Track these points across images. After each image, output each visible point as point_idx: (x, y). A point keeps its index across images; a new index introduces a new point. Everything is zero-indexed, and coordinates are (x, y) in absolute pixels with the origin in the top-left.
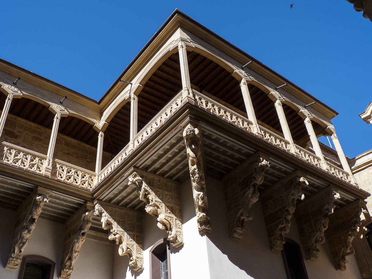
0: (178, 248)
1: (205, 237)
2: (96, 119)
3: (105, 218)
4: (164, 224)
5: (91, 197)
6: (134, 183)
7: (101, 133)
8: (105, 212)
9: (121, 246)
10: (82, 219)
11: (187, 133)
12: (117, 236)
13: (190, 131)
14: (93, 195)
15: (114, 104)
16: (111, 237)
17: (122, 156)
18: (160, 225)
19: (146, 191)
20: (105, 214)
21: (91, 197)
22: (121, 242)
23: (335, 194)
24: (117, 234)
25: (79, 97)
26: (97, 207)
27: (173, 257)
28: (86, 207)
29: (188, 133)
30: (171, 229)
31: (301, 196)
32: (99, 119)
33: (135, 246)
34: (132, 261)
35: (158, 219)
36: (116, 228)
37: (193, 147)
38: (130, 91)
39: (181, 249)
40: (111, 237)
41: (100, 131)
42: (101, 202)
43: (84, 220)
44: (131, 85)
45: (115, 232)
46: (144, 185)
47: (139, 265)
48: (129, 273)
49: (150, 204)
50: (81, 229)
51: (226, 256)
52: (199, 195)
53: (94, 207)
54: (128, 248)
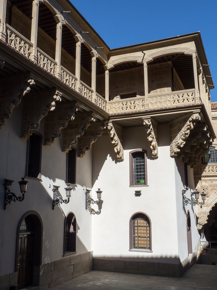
0: (155, 157)
1: (173, 159)
2: (106, 61)
3: (113, 132)
4: (153, 146)
5: (108, 118)
6: (147, 125)
7: (107, 72)
8: (114, 128)
12: (117, 142)
14: (110, 117)
18: (151, 147)
19: (151, 129)
20: (113, 129)
21: (108, 118)
22: (117, 145)
24: (117, 141)
25: (104, 45)
26: (110, 125)
27: (149, 162)
28: (104, 123)
29: (196, 118)
30: (154, 149)
31: (204, 142)
32: (107, 60)
33: (122, 148)
34: (120, 156)
35: (152, 144)
36: (116, 138)
37: (195, 124)
38: (143, 58)
39: (156, 159)
41: (107, 70)
42: (113, 122)
43: (100, 130)
44: (143, 54)
46: (151, 127)
47: (122, 158)
48: (109, 158)
49: (151, 136)
50: (97, 134)
51: (177, 167)
52: (183, 142)
53: (108, 123)
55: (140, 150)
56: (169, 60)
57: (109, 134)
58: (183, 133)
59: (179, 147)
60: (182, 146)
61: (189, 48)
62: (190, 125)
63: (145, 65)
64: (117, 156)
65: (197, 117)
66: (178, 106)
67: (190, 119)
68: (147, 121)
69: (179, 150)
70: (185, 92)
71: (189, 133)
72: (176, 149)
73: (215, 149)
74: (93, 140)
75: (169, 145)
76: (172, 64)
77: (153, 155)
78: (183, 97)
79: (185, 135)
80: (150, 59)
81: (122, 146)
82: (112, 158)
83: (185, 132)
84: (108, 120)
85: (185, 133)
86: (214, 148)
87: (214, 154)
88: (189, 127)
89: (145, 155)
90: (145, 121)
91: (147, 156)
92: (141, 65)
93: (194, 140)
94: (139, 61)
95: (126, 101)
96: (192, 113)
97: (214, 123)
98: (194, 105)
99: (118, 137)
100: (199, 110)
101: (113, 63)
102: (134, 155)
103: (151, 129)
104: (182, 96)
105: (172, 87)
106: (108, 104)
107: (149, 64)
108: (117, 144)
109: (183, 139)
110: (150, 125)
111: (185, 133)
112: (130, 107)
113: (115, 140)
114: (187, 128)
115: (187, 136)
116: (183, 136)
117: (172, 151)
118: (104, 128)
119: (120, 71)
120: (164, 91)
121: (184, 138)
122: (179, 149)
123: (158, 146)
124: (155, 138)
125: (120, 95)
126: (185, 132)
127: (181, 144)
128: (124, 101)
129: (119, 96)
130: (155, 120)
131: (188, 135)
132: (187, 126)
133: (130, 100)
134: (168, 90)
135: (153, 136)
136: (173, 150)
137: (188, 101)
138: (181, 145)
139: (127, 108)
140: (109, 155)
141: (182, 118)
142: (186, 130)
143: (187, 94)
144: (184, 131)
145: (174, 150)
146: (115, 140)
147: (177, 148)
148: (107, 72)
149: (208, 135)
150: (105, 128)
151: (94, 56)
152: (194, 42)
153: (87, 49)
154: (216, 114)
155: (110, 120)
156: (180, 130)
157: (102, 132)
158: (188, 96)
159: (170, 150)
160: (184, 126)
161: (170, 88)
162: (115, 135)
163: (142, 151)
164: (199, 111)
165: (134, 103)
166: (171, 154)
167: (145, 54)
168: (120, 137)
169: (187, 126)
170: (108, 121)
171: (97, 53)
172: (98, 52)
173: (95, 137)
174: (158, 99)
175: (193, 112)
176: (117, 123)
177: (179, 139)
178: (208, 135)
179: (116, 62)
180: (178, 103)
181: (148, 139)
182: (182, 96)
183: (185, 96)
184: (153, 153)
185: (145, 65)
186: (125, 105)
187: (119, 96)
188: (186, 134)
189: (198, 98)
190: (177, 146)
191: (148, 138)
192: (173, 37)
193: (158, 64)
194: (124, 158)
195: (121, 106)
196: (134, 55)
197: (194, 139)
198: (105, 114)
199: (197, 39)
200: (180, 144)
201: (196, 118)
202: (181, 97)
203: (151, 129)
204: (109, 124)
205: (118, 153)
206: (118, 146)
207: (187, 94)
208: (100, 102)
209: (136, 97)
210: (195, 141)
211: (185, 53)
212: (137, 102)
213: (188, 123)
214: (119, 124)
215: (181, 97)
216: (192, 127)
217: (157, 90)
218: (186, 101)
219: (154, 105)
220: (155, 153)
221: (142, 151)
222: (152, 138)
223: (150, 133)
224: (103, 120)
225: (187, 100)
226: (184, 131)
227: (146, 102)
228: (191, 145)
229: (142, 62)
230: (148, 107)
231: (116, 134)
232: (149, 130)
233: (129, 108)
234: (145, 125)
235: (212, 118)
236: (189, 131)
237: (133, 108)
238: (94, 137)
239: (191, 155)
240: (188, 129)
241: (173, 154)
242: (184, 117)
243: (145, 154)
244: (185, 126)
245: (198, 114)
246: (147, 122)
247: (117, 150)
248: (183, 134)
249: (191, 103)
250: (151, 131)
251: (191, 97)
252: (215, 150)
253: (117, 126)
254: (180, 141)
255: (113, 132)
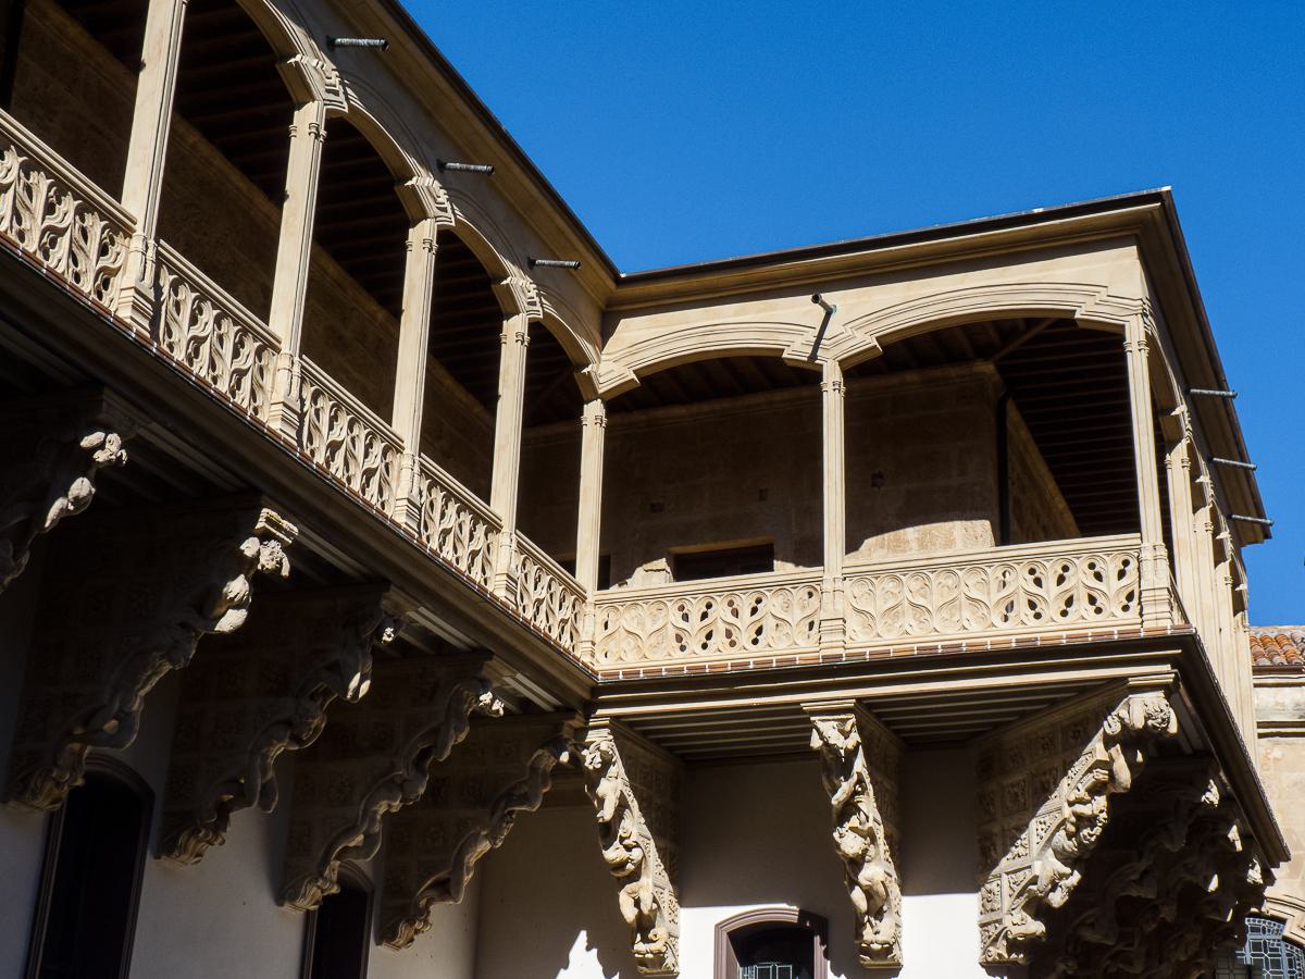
3: (613, 787)
4: (869, 893)
5: (586, 696)
7: (593, 412)
8: (620, 762)
9: (628, 887)
10: (529, 764)
11: (1148, 717)
12: (636, 854)
13: (1163, 720)
14: (597, 690)
15: (711, 329)
16: (613, 854)
17: (757, 596)
18: (858, 896)
19: (860, 781)
20: (617, 769)
22: (635, 876)
23: (1253, 868)
24: (638, 846)
26: (600, 740)
28: (558, 727)
29: (1150, 722)
31: (1208, 881)
32: (599, 340)
33: (666, 892)
36: (634, 825)
37: (1140, 758)
40: (613, 854)
41: (596, 396)
42: (618, 726)
43: (534, 769)
44: (823, 313)
45: (633, 838)
46: (860, 764)
47: (669, 961)
49: (854, 821)
50: (511, 797)
52: (1062, 876)
53: (585, 730)
54: (655, 901)
55: (784, 911)
56: (983, 352)
57: (591, 803)
58: (1067, 812)
59: (1037, 907)
60: (1057, 899)
61: (1106, 285)
62: (1107, 765)
63: (832, 376)
64: (636, 947)
65: (1151, 711)
66: (1029, 640)
67: (1112, 726)
68: (835, 724)
69: (1037, 927)
70: (1078, 553)
71: (1104, 815)
72: (1019, 915)
73: (1286, 933)
74: (484, 833)
75: (976, 889)
76: (997, 377)
77: (868, 951)
78: (1065, 586)
79: (1078, 829)
80: (863, 340)
81: (672, 881)
82: (601, 958)
83: (1079, 808)
84: (589, 708)
85: (1075, 814)
86: (1275, 926)
87: (1277, 964)
88: (1101, 775)
89: (819, 950)
90: (820, 725)
91: (826, 955)
92: (808, 376)
93: (1143, 865)
94: (796, 348)
95: (706, 592)
96: (1119, 690)
97: (1276, 759)
98: (1134, 636)
99: (643, 820)
100: (1165, 672)
101: (637, 357)
102: (746, 944)
103: (855, 777)
104: (1061, 580)
105: (997, 520)
106: (588, 608)
107: (857, 370)
108: (639, 866)
109: (1062, 856)
110: (852, 754)
111: (1079, 817)
112: (729, 634)
113: (626, 842)
114: (1089, 780)
115: (1090, 834)
116: (1062, 833)
117: (993, 931)
118: (558, 757)
119: (679, 411)
120: (950, 543)
121: (1070, 845)
122: (1036, 917)
123: (904, 892)
124: (881, 840)
125: (669, 553)
126: (1079, 808)
127: (1054, 886)
128: (694, 594)
129: (662, 563)
130: (888, 724)
131: (1098, 830)
132: (1090, 770)
133: (732, 590)
134: (970, 536)
135: (871, 824)
136: (999, 921)
137: (1098, 611)
138: (1053, 889)
139: (709, 636)
140: (583, 937)
141: (1057, 717)
142: (1083, 794)
143: (1092, 566)
144: (1072, 798)
145: (1007, 921)
146: (626, 842)
147: (1025, 908)
148: (593, 412)
149: (1233, 834)
150: (564, 758)
151: (518, 313)
152: (1135, 247)
153: (478, 268)
154: (1283, 705)
155: (600, 712)
156: (1044, 791)
157: (545, 786)
158: (1098, 576)
159: (983, 925)
160: (1068, 765)
161: (987, 523)
162: (628, 806)
163: (794, 919)
164: (1170, 679)
165: (754, 611)
166: (985, 951)
167: (829, 312)
168: (659, 826)
169: (1090, 770)
170: (587, 718)
171: (533, 293)
172: (540, 285)
173: (498, 814)
174: (906, 589)
175: (1124, 679)
176: (645, 733)
177: (1035, 849)
178: (1233, 834)
179: (653, 355)
180: (1033, 622)
181: (838, 846)
182: (1061, 580)
183: (1080, 577)
184: (868, 934)
185: (832, 376)
186: (695, 617)
187: (662, 563)
188: (1083, 821)
189: (1157, 592)
190: (1023, 900)
191: (836, 835)
192: (1003, 216)
193: (911, 377)
194: (680, 960)
195: (670, 626)
196: (762, 315)
197: (1140, 856)
198: (568, 673)
199: (1157, 239)
200: (1043, 883)
201: (1150, 722)
202: (1050, 581)
203: (860, 781)
204: (592, 736)
205: (644, 925)
206: (644, 880)
207: (1092, 566)
208: (544, 594)
209: (770, 568)
210: (1145, 873)
211: (1077, 316)
212: (772, 604)
213: (1096, 749)
214: (658, 741)
215: (1050, 581)
216: (1124, 775)
217: (902, 531)
218: (1082, 606)
219: (880, 628)
220: (880, 938)
221: (794, 919)
222: (863, 836)
223: (850, 807)
224: (557, 708)
225: (1092, 600)
226: (1071, 804)
227: (832, 605)
228: (1123, 894)
229: (814, 356)
230: (840, 637)
231: (634, 804)
232: (845, 788)
233: (719, 639)
234: (818, 752)
235: (1260, 725)
236: (1101, 802)
237: (744, 638)
238: (493, 814)
239: (1121, 966)
240: (1095, 790)
241: (1001, 949)
242: (1071, 712)
243: (817, 939)
244: (1080, 766)
245: (1161, 694)
246: (832, 733)
247: (637, 903)
248: (1063, 823)
249: (1115, 622)
250: (855, 793)
251: (1112, 586)
252: (1286, 939)
253: (641, 750)
254: (1047, 866)
255: (613, 787)
